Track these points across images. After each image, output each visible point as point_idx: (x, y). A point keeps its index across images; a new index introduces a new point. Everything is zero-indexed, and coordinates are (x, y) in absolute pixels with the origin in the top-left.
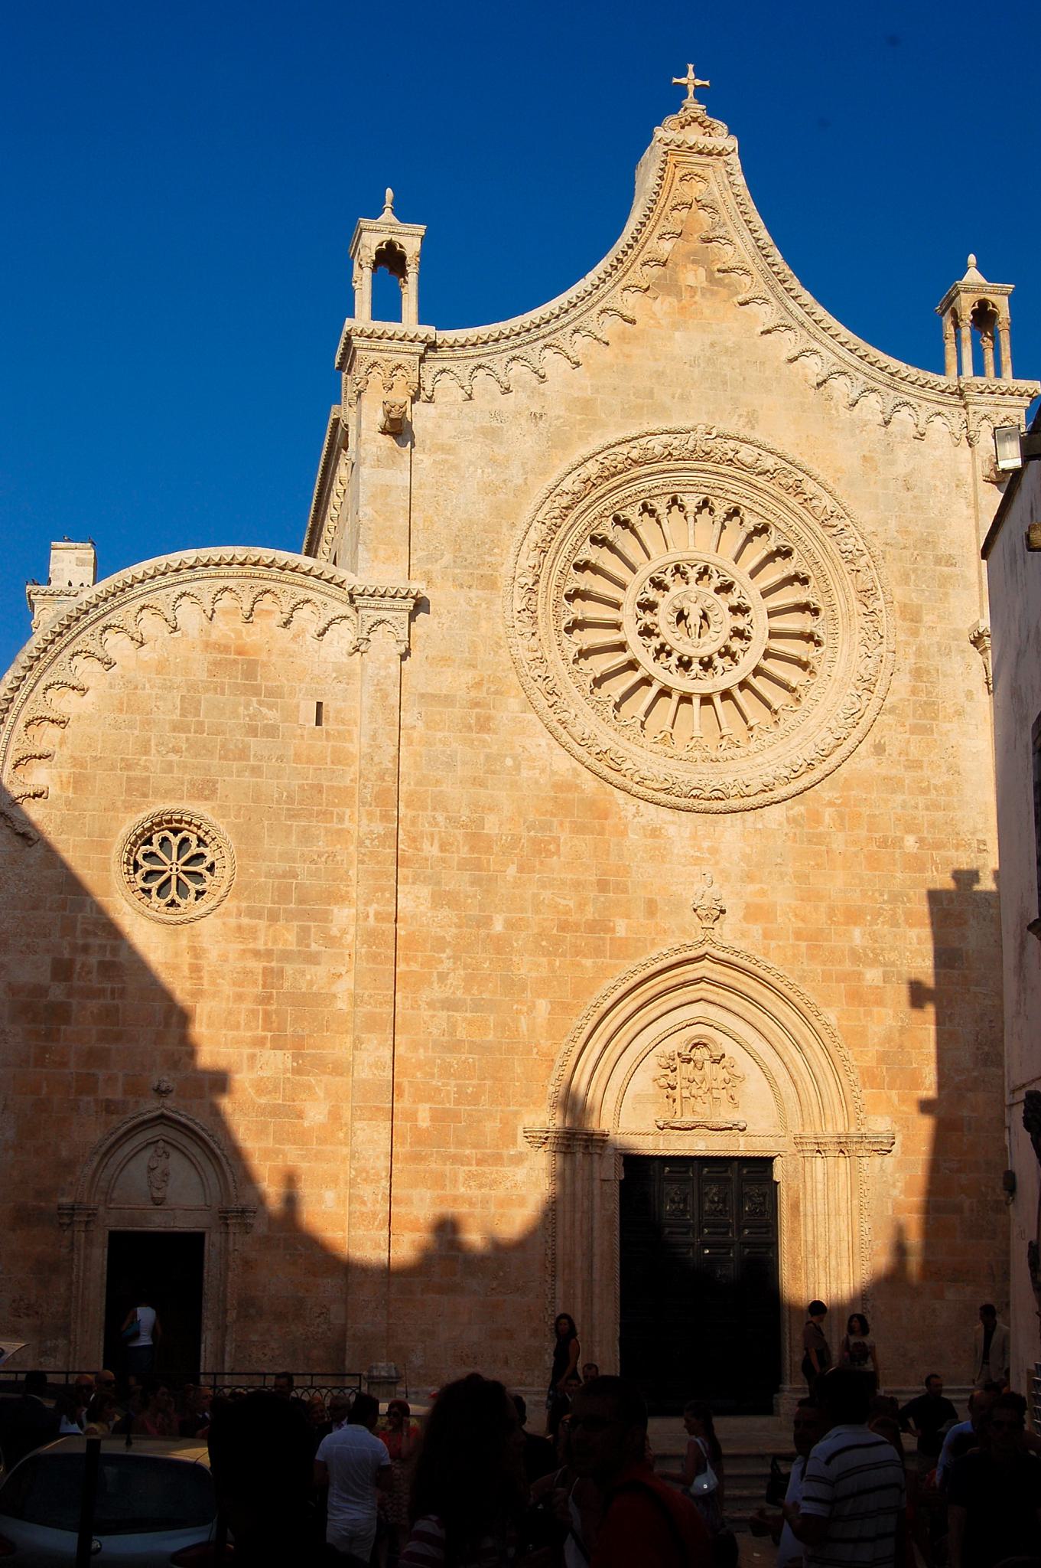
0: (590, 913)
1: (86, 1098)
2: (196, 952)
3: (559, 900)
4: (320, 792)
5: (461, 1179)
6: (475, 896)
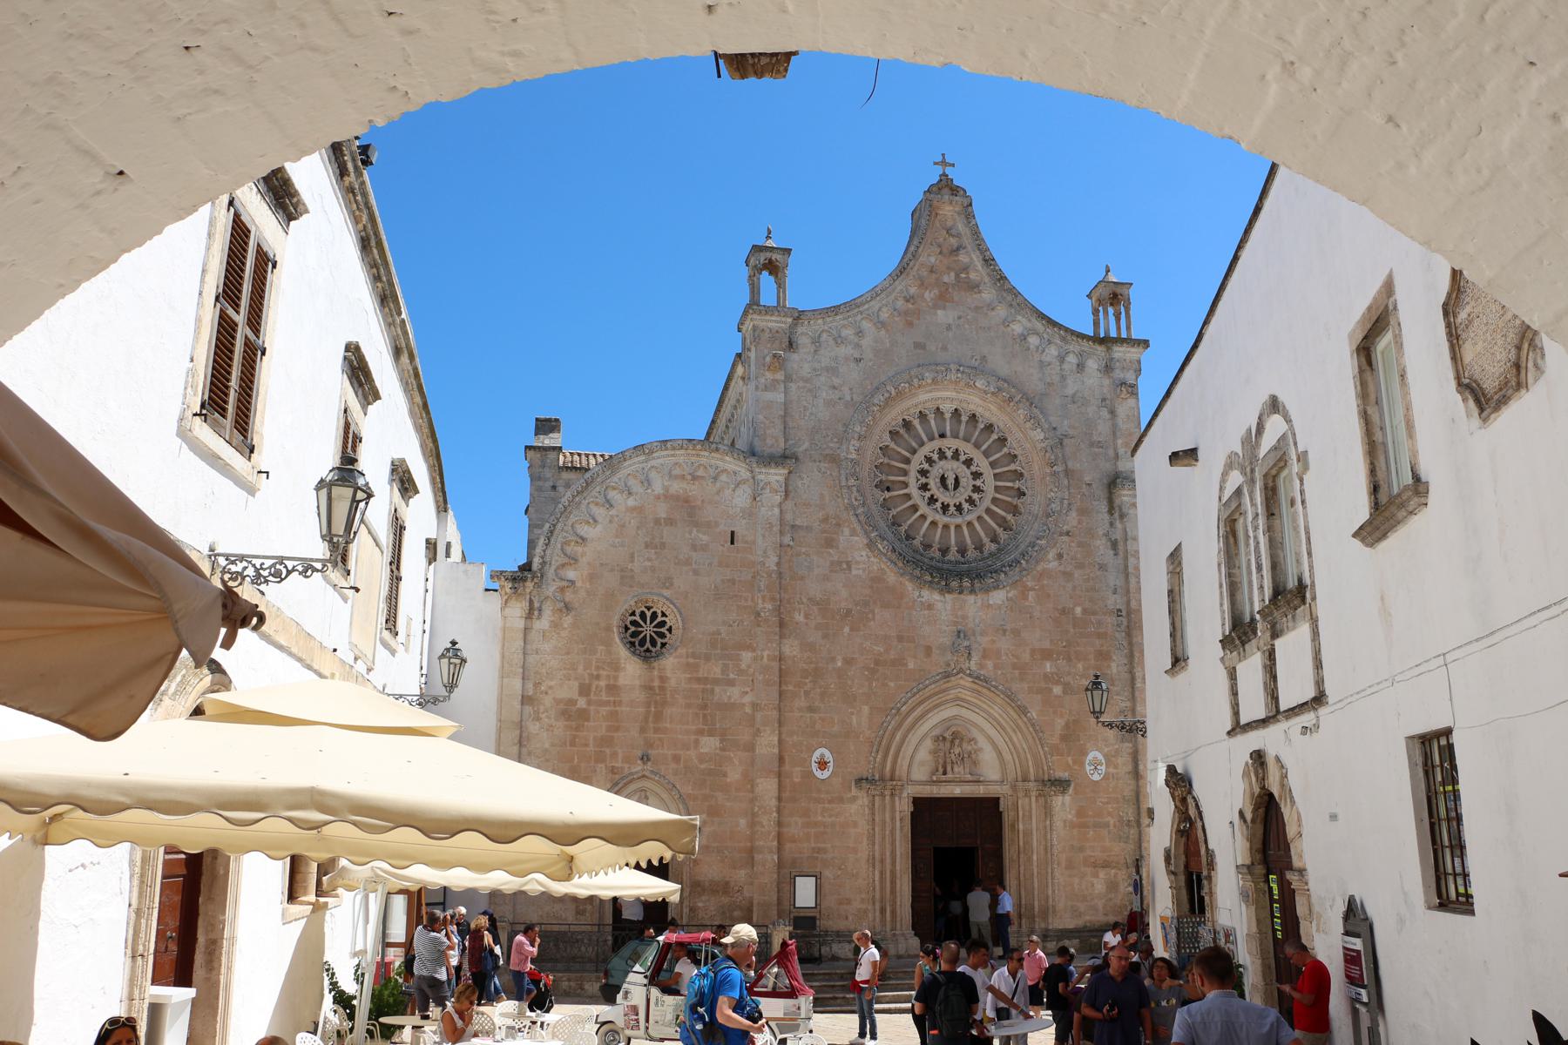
0: (892, 655)
1: (600, 765)
2: (663, 679)
3: (875, 647)
4: (734, 584)
5: (819, 811)
6: (825, 645)
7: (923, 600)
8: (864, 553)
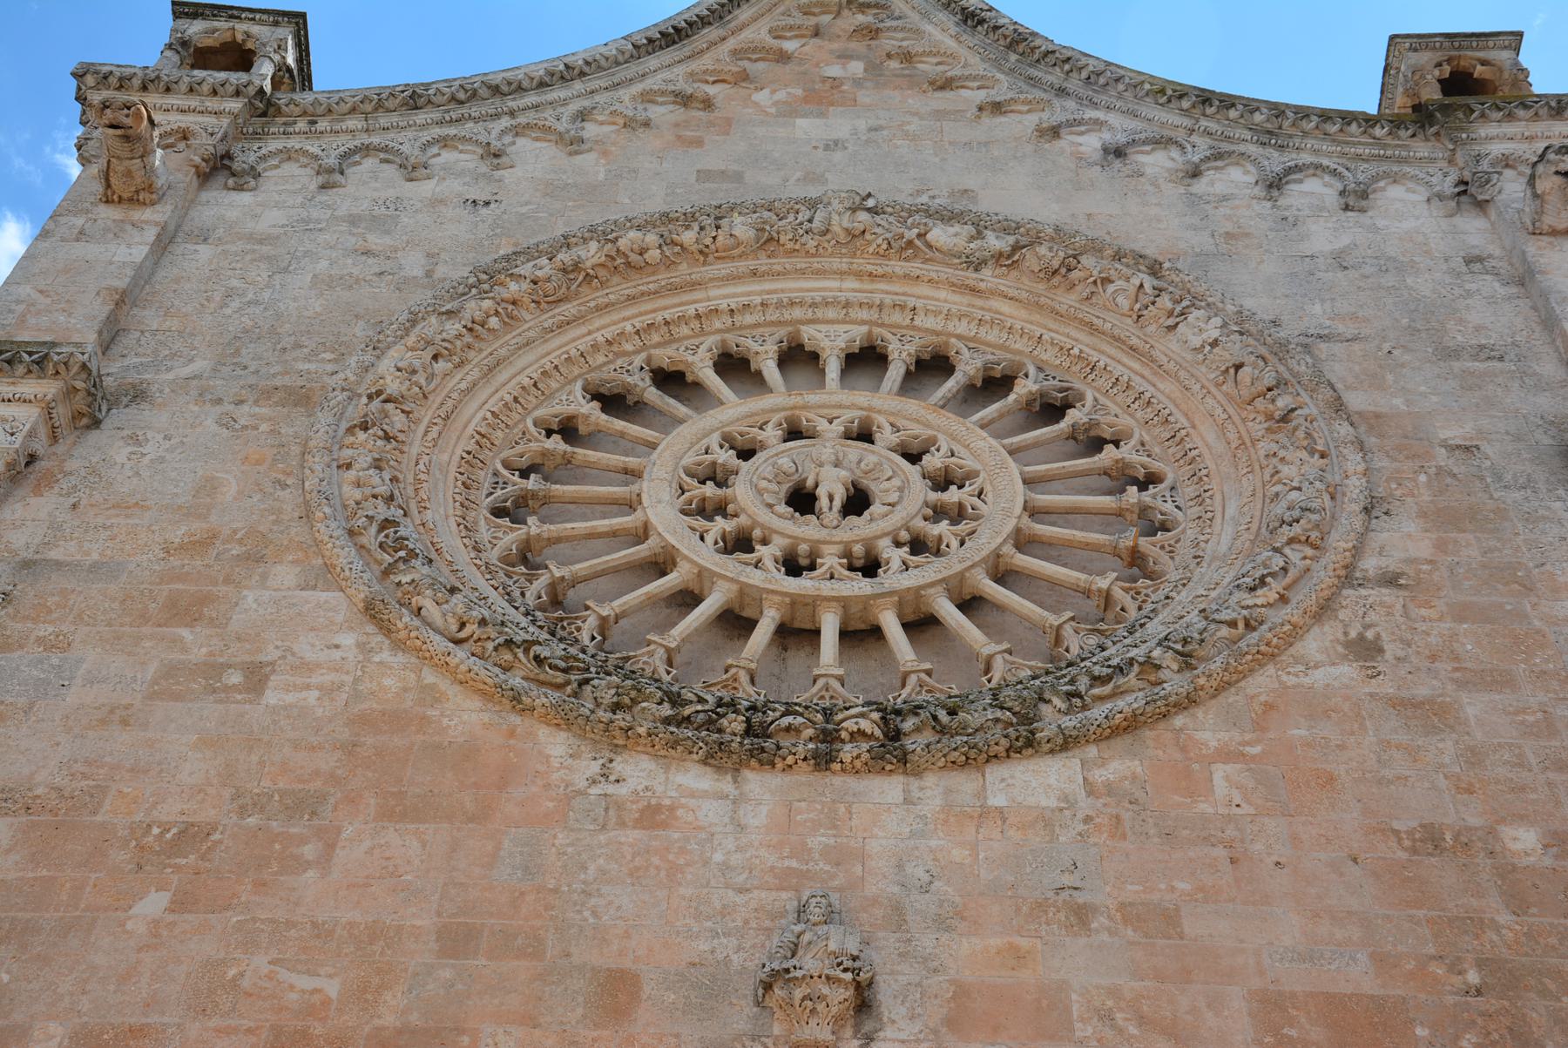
7: (622, 790)
8: (348, 640)
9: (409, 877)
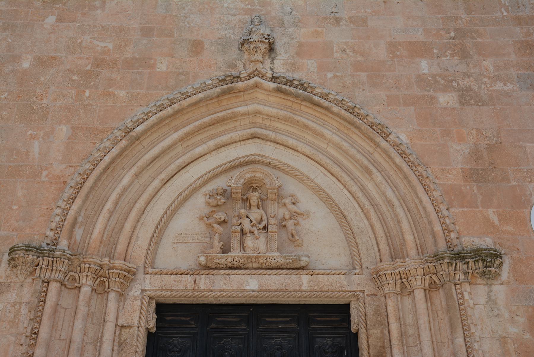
0: (129, 53)
9: (130, 12)
